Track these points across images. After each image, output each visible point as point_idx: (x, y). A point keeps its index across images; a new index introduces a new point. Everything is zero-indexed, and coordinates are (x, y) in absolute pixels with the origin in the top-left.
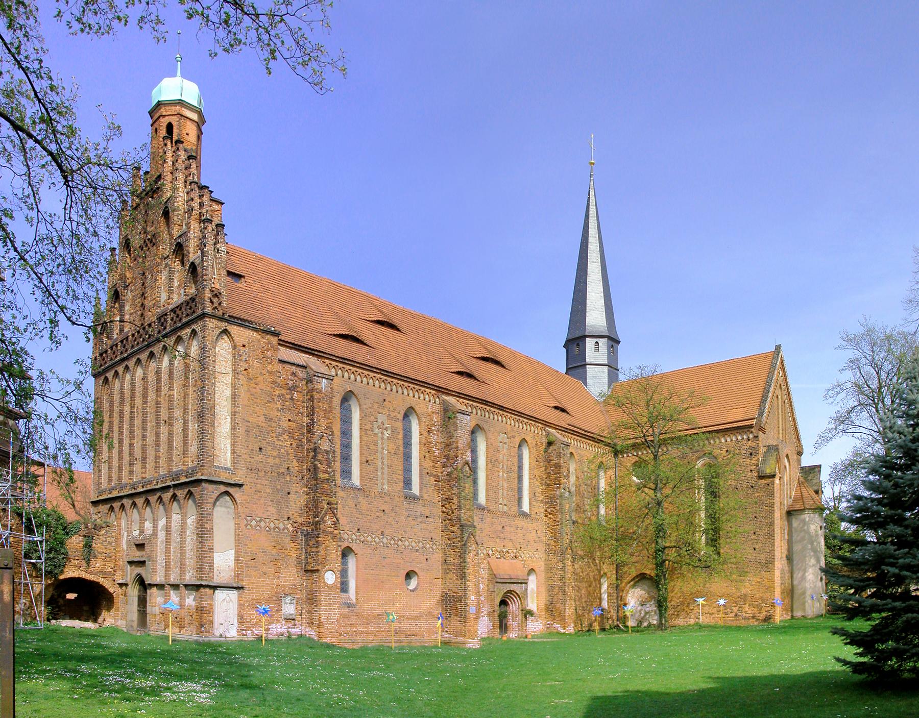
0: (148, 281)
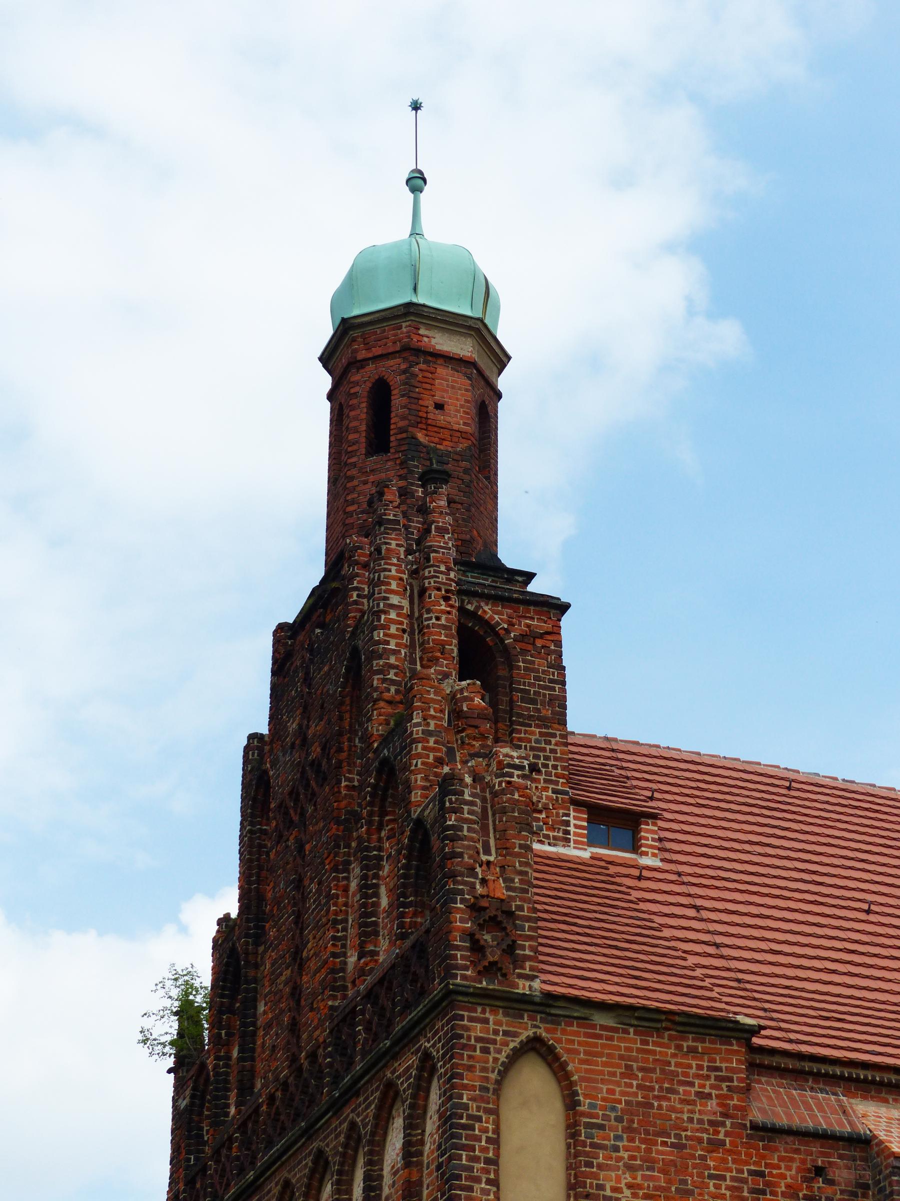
0: (311, 904)
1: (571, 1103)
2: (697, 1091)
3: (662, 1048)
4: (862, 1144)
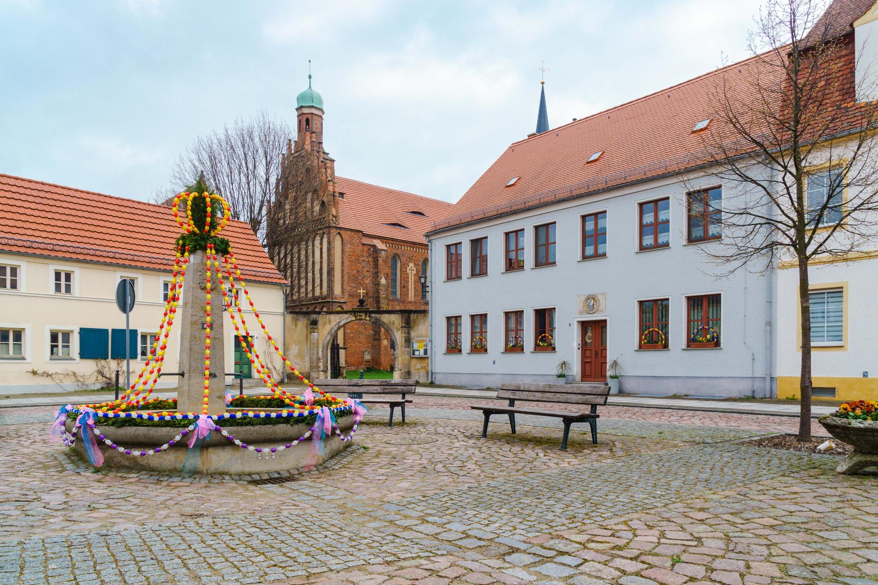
1: (342, 240)
2: (356, 237)
3: (353, 233)
4: (374, 246)
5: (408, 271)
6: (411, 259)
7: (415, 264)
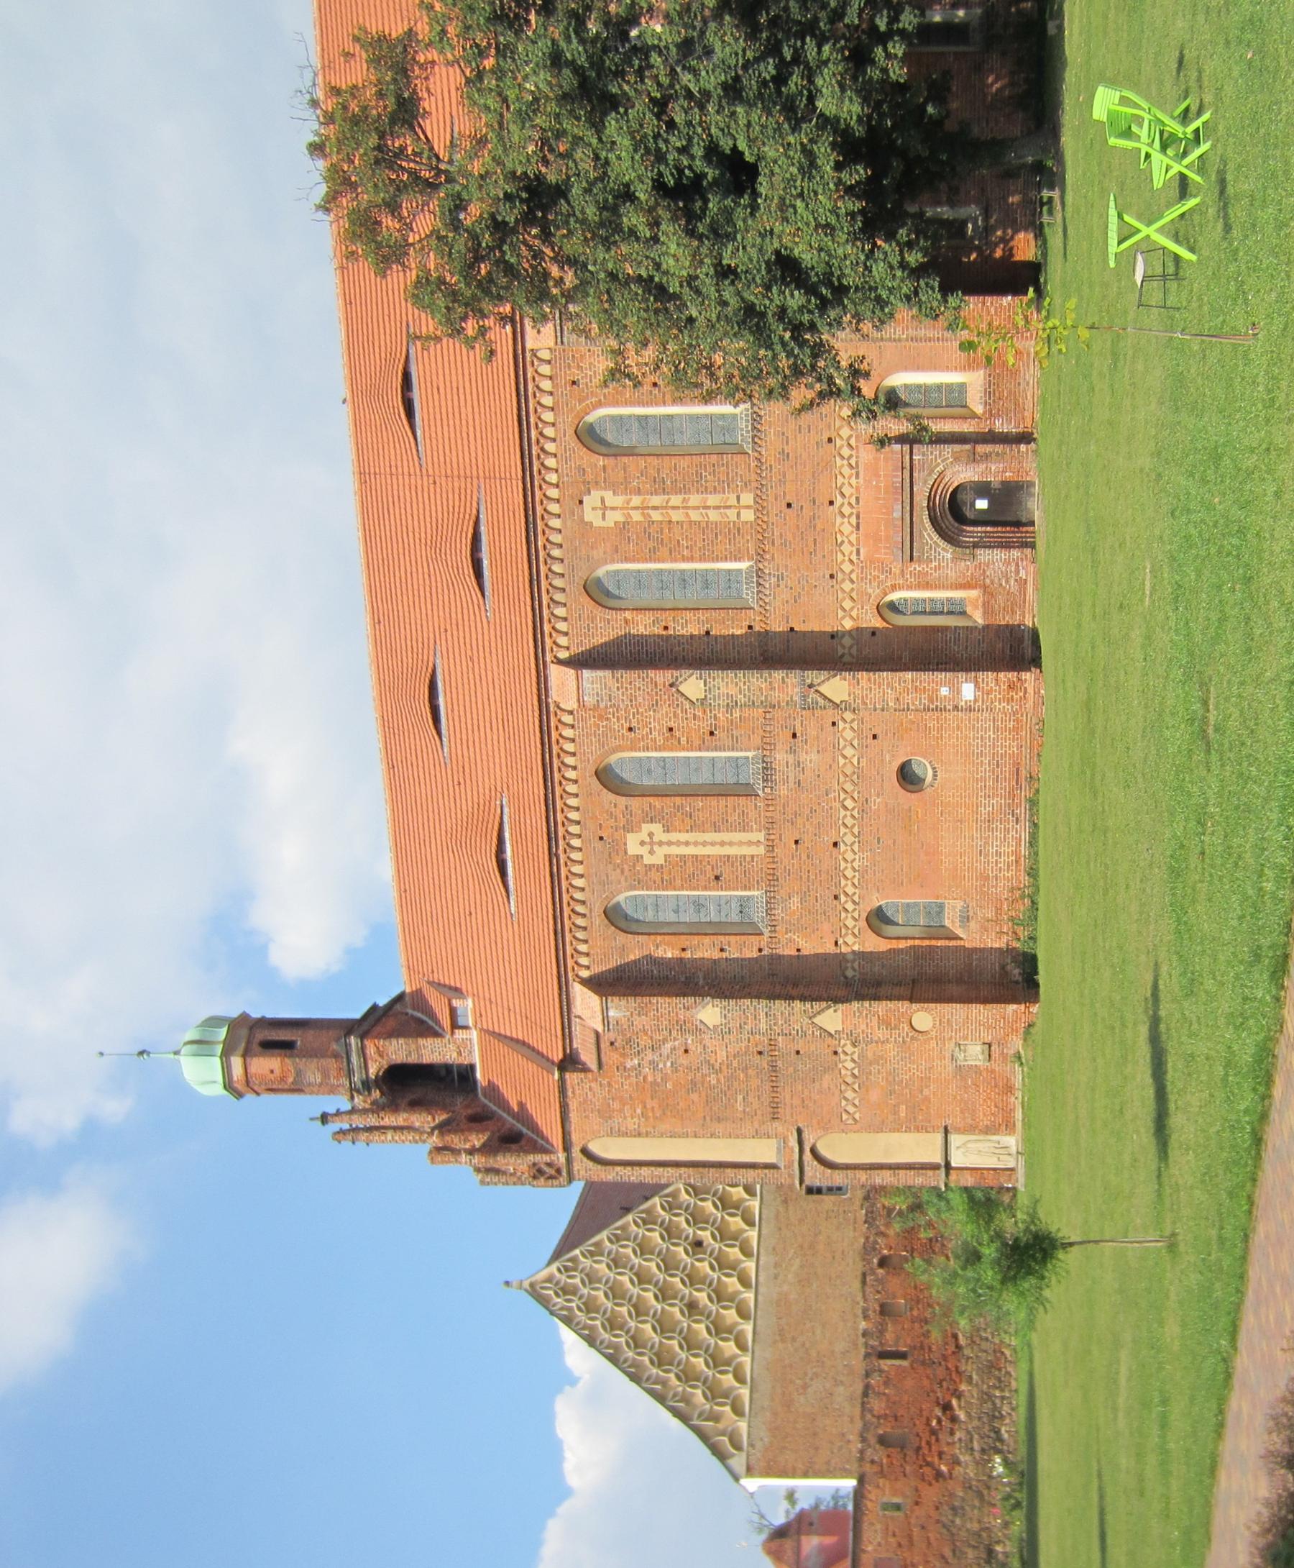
5: (658, 859)
6: (611, 847)
7: (630, 827)
